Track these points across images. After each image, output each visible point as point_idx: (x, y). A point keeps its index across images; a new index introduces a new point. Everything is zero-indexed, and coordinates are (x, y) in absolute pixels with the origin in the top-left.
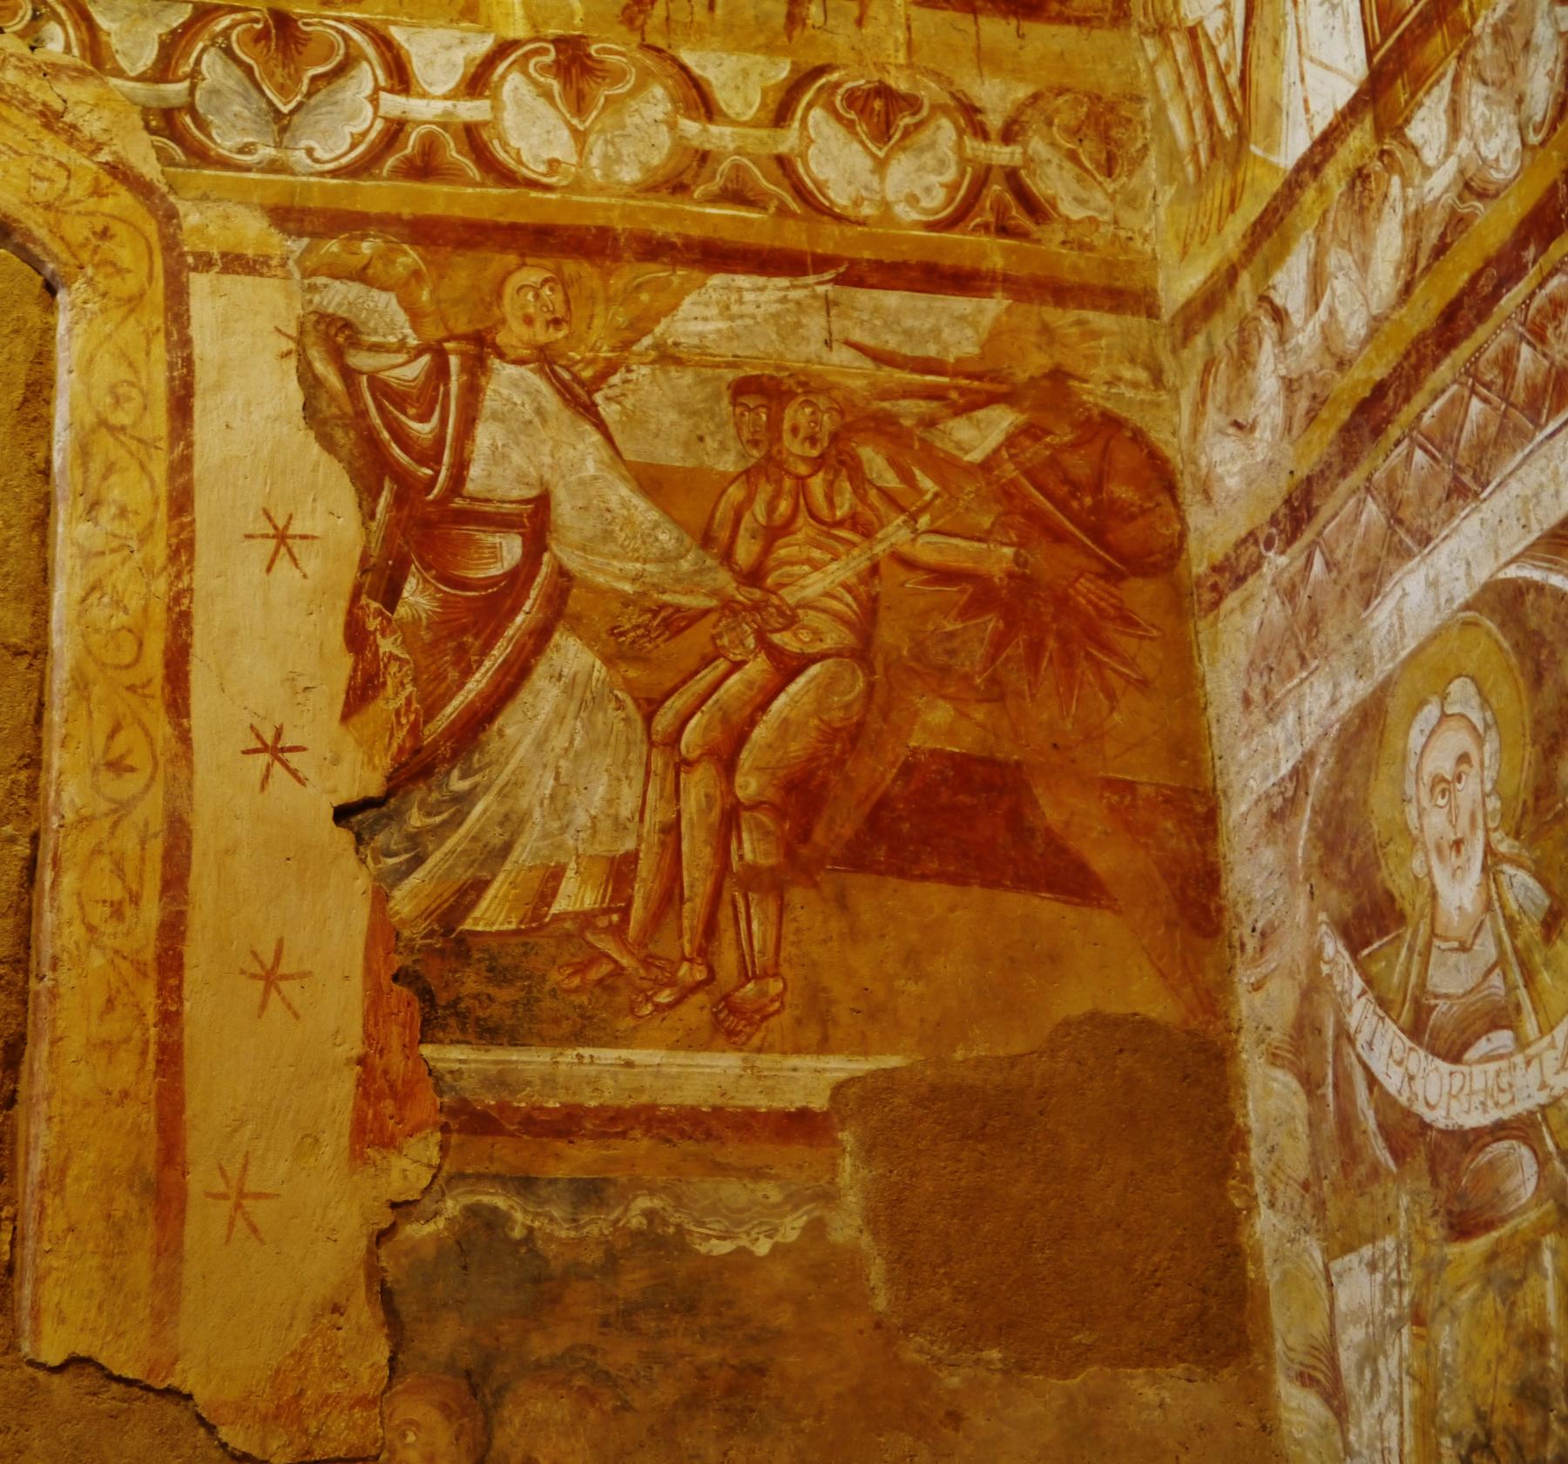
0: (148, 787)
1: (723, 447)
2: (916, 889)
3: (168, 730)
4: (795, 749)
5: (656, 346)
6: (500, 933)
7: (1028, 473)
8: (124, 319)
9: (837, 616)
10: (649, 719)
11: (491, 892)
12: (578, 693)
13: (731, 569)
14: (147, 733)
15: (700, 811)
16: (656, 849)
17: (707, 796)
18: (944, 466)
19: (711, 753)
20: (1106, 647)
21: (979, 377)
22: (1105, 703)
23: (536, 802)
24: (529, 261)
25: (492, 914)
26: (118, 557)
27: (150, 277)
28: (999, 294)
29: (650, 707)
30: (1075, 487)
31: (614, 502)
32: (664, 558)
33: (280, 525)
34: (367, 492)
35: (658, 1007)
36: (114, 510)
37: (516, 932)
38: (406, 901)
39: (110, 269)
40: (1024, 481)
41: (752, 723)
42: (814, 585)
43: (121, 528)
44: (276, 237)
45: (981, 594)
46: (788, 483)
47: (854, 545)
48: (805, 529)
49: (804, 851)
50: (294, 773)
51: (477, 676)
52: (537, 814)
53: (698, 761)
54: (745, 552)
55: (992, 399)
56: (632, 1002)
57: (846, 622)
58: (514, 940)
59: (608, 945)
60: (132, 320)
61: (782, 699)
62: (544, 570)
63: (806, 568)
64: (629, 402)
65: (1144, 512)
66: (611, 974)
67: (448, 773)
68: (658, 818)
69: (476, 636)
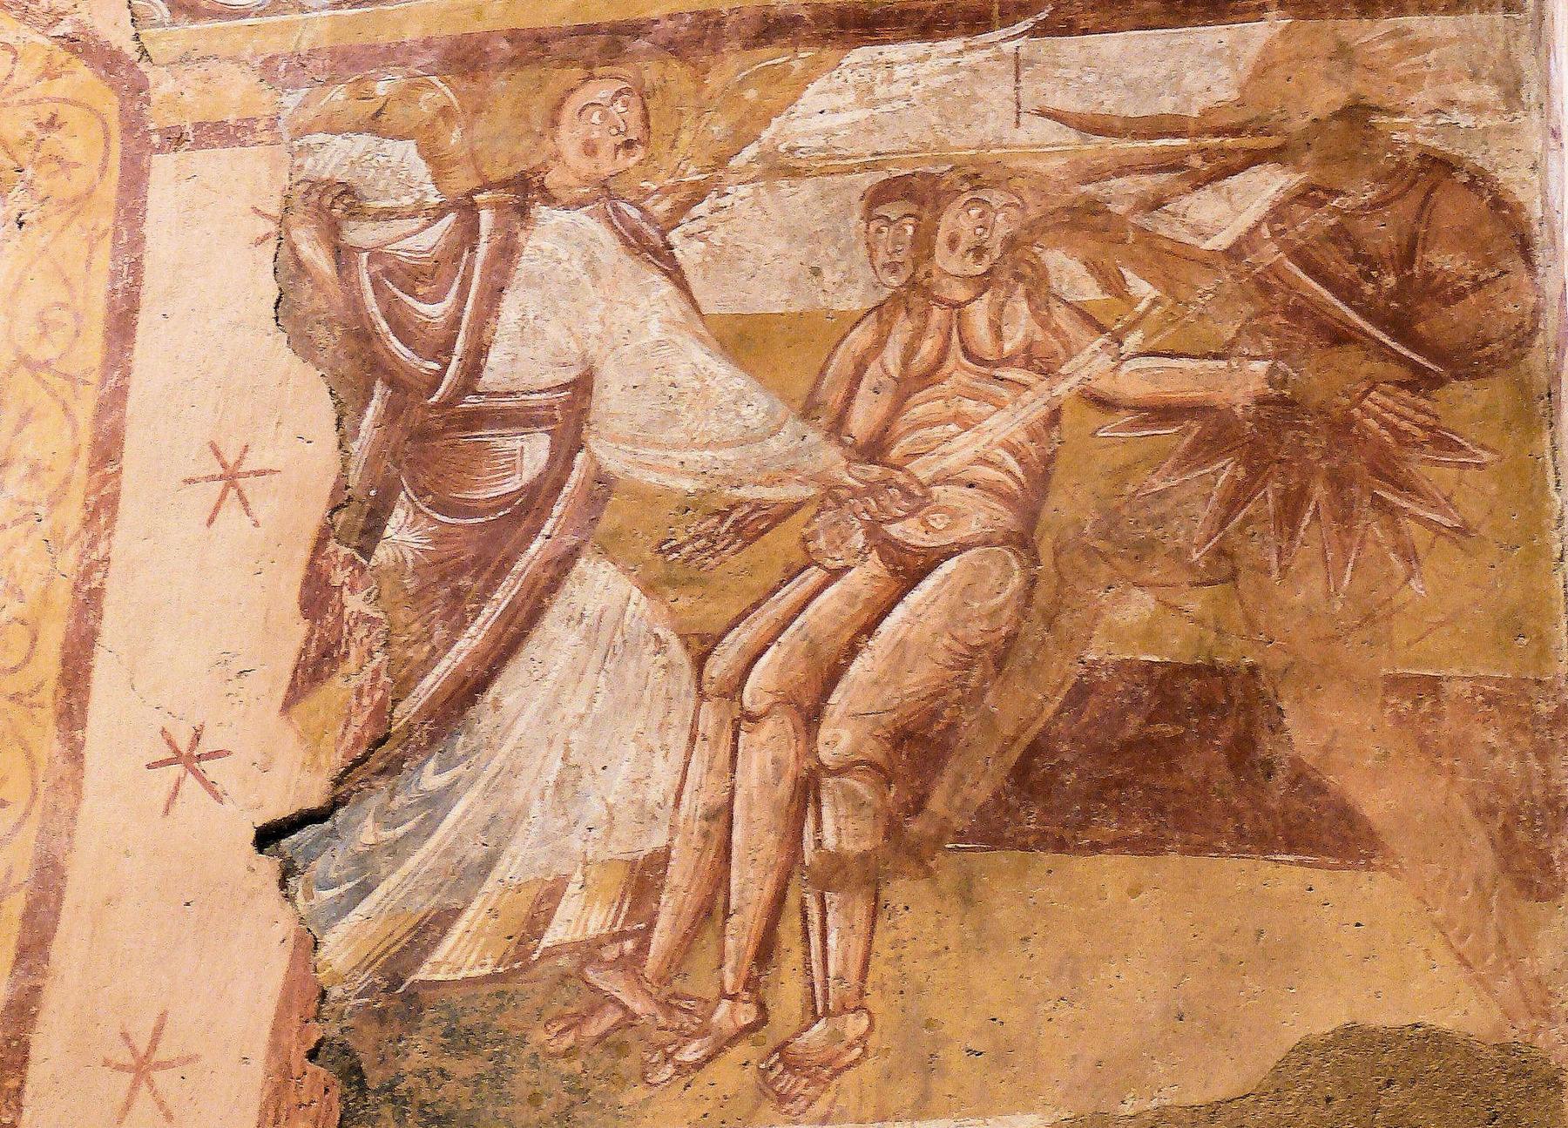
0: (19, 825)
1: (849, 280)
2: (1080, 865)
3: (56, 746)
4: (919, 678)
5: (761, 157)
6: (467, 981)
7: (1298, 255)
8: (66, 225)
9: (991, 489)
10: (700, 662)
11: (461, 925)
12: (604, 638)
13: (841, 443)
14: (29, 755)
15: (764, 784)
16: (696, 841)
17: (775, 761)
18: (1169, 261)
19: (787, 699)
20: (1405, 486)
21: (1236, 132)
22: (1399, 567)
23: (535, 793)
24: (598, 71)
25: (459, 957)
26: (20, 529)
27: (104, 168)
28: (1272, 14)
29: (702, 649)
30: (1369, 264)
31: (682, 373)
32: (746, 439)
33: (231, 461)
34: (347, 403)
35: (679, 1066)
36: (24, 469)
37: (488, 979)
38: (342, 949)
39: (54, 166)
40: (1289, 264)
41: (852, 651)
42: (961, 450)
43: (28, 492)
44: (266, 98)
45: (1212, 430)
46: (937, 314)
47: (1027, 387)
48: (958, 372)
49: (915, 827)
50: (209, 786)
51: (472, 630)
52: (535, 809)
53: (766, 714)
54: (862, 420)
55: (1256, 158)
56: (645, 1063)
57: (1006, 498)
58: (486, 990)
59: (614, 984)
60: (75, 226)
61: (899, 612)
62: (575, 476)
63: (953, 428)
64: (716, 238)
65: (1478, 285)
66: (616, 1027)
67: (421, 765)
68: (703, 798)
69: (476, 577)
